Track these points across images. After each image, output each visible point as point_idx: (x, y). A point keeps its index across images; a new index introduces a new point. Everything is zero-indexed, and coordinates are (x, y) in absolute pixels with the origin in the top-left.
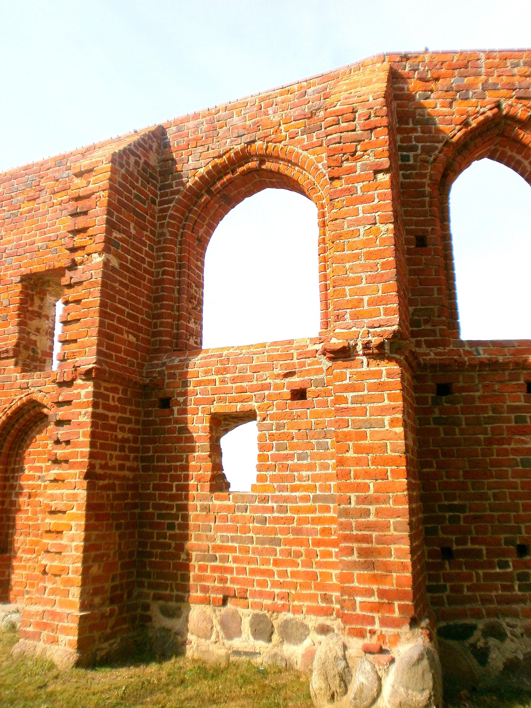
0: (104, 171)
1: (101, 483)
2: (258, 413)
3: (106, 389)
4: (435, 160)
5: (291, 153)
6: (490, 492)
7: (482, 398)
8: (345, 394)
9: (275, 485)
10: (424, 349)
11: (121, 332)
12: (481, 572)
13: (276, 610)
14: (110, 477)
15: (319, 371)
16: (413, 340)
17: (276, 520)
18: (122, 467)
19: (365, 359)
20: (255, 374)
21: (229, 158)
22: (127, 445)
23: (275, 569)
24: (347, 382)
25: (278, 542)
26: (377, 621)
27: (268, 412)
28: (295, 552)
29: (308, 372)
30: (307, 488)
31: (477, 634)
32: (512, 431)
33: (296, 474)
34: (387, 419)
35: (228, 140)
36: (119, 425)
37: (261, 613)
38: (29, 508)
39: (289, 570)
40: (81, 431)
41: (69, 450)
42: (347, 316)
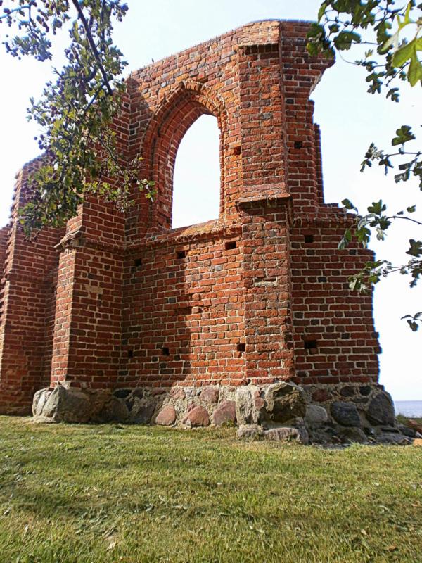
1: (15, 330)
3: (19, 284)
4: (147, 129)
6: (153, 319)
7: (154, 265)
10: (130, 241)
11: (32, 255)
12: (144, 364)
14: (22, 328)
16: (126, 237)
18: (30, 324)
22: (35, 313)
31: (131, 394)
32: (168, 283)
36: (29, 303)
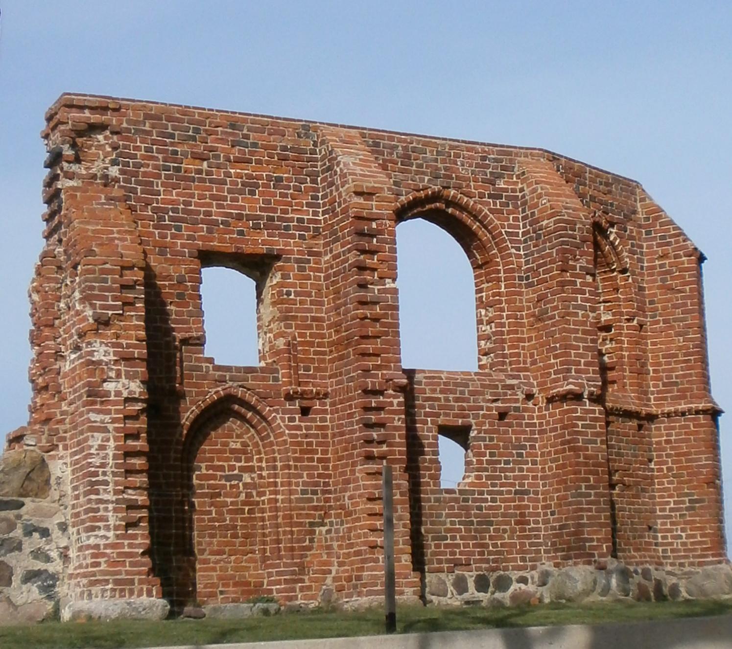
0: (389, 200)
2: (474, 427)
5: (481, 211)
8: (578, 422)
9: (489, 482)
13: (494, 570)
15: (517, 401)
17: (490, 508)
19: (587, 401)
20: (472, 398)
21: (427, 196)
23: (490, 542)
24: (579, 414)
25: (491, 523)
26: (596, 555)
27: (483, 428)
28: (503, 529)
29: (509, 401)
30: (513, 485)
33: (503, 474)
34: (599, 440)
35: (426, 178)
37: (482, 573)
38: (212, 508)
39: (499, 542)
40: (397, 433)
41: (385, 448)
42: (573, 371)
